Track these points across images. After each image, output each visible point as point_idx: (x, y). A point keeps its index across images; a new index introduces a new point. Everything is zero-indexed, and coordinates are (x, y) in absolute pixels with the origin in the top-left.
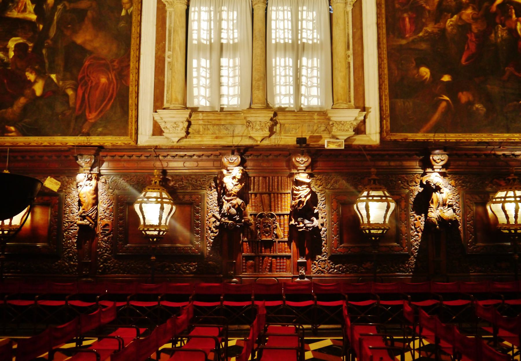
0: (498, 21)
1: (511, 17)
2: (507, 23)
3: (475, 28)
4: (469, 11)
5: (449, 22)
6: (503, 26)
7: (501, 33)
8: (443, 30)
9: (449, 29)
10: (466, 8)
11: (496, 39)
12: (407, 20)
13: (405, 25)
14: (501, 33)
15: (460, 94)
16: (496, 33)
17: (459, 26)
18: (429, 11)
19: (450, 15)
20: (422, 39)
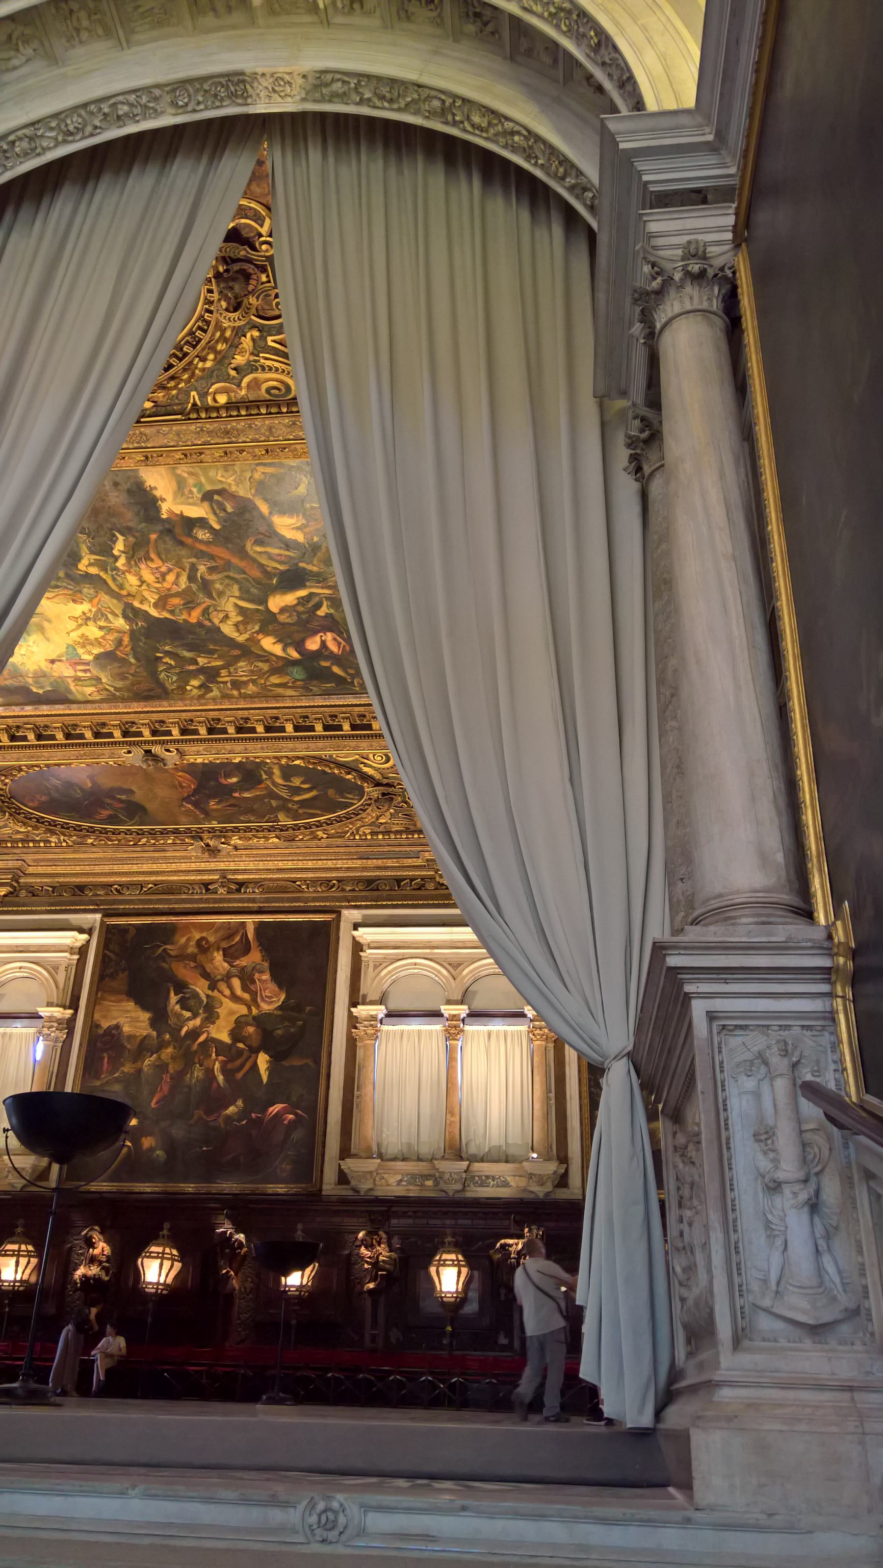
0: (196, 1060)
1: (211, 1056)
2: (205, 1063)
3: (171, 1070)
4: (170, 1050)
5: (147, 1062)
6: (201, 1065)
7: (198, 1073)
8: (139, 1071)
9: (145, 1069)
10: (166, 1048)
11: (191, 1080)
12: (106, 1059)
13: (102, 1065)
14: (198, 1073)
15: (144, 1139)
16: (192, 1073)
17: (157, 1066)
18: (129, 1051)
19: (149, 1054)
20: (117, 1080)
